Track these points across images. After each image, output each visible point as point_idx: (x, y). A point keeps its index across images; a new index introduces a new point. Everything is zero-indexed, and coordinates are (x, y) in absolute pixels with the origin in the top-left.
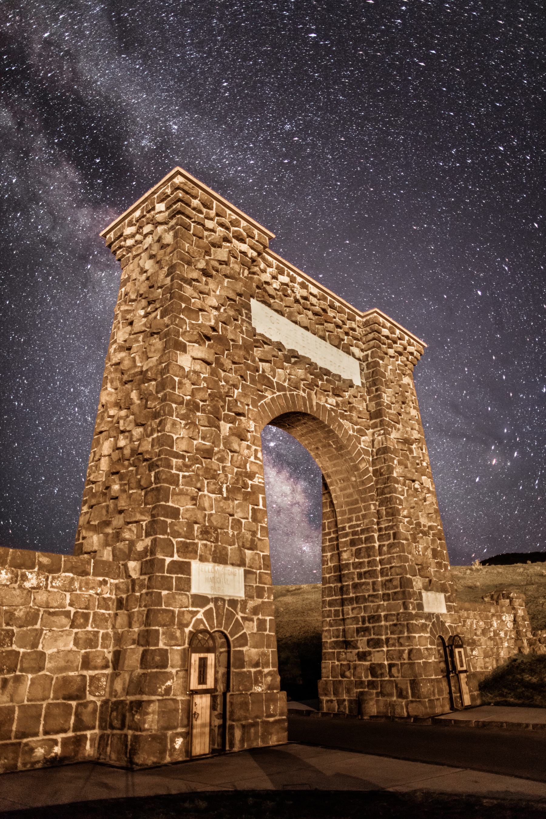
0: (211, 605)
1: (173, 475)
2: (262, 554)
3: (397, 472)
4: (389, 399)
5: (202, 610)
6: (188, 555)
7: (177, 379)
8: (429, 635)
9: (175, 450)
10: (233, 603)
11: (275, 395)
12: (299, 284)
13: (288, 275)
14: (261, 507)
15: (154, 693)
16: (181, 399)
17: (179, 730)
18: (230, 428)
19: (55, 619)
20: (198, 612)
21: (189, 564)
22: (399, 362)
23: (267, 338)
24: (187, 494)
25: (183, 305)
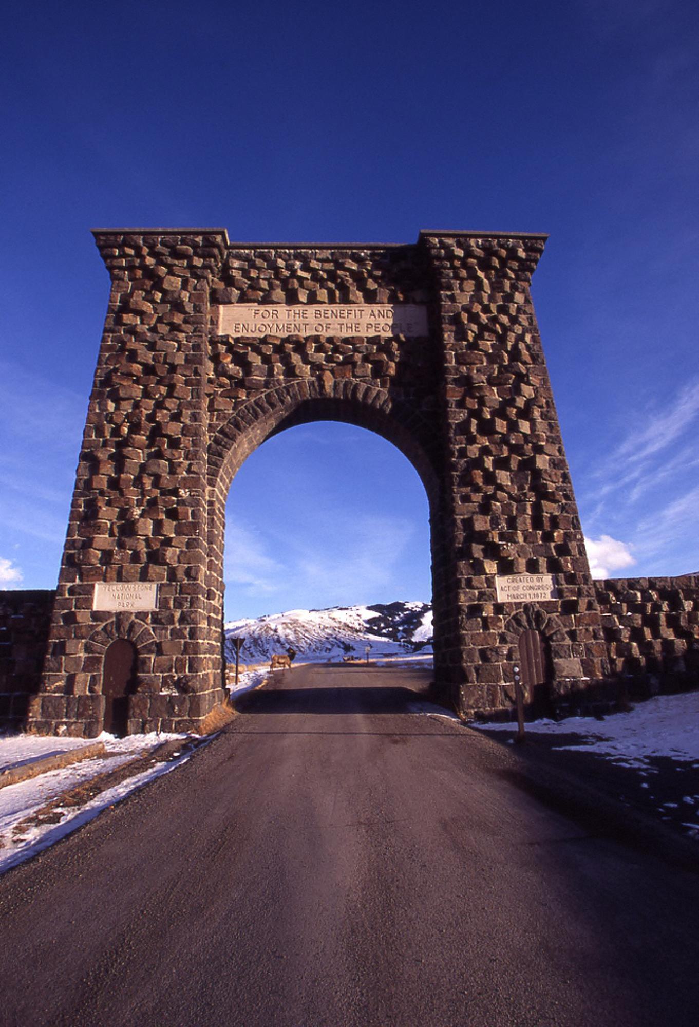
0: (114, 619)
5: (104, 624)
6: (91, 578)
8: (503, 630)
10: (142, 615)
14: (190, 519)
15: (46, 691)
16: (96, 443)
17: (64, 720)
20: (99, 625)
21: (93, 586)
23: (248, 338)
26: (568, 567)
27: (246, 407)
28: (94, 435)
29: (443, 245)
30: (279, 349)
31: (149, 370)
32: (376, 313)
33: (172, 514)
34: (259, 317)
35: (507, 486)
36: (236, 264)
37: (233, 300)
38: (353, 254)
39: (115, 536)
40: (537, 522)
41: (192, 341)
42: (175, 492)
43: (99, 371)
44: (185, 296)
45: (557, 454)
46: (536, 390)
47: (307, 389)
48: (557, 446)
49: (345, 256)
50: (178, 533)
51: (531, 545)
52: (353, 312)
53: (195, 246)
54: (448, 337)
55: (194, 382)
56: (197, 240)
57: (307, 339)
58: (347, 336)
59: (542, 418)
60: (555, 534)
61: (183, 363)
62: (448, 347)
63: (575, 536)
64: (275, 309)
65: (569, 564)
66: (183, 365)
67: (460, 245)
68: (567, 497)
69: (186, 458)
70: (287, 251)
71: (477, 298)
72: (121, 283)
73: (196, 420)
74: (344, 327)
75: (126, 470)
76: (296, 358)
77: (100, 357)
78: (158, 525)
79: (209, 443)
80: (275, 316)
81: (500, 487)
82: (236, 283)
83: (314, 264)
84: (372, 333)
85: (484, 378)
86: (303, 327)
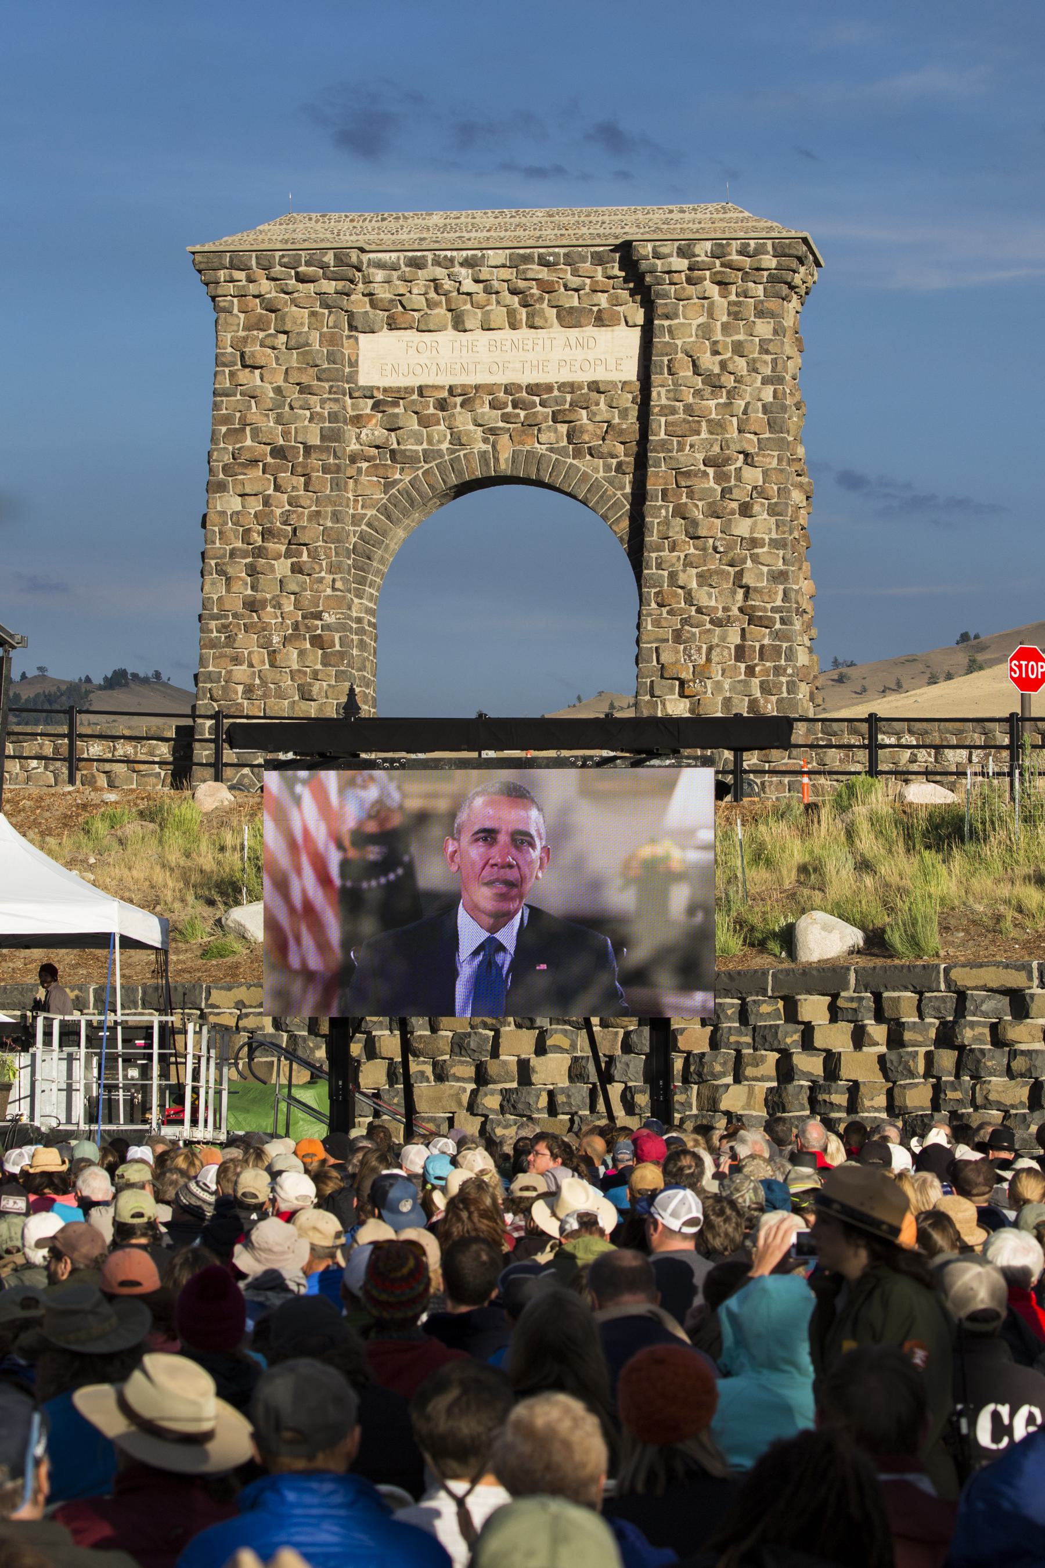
1: (211, 640)
2: (335, 702)
3: (659, 531)
4: (671, 395)
7: (216, 529)
9: (215, 611)
11: (420, 472)
12: (461, 265)
13: (437, 263)
14: (338, 648)
16: (222, 551)
18: (292, 564)
19: (146, 779)
22: (733, 297)
23: (398, 390)
24: (226, 656)
25: (224, 429)
26: (766, 707)
27: (398, 490)
28: (217, 541)
29: (657, 256)
30: (442, 405)
31: (278, 452)
32: (573, 342)
33: (317, 641)
34: (412, 352)
35: (707, 607)
36: (379, 275)
37: (376, 328)
38: (540, 256)
39: (253, 666)
40: (740, 653)
41: (327, 406)
42: (318, 616)
43: (215, 453)
44: (315, 337)
45: (781, 561)
46: (765, 473)
47: (476, 463)
48: (781, 553)
49: (527, 259)
50: (324, 664)
51: (729, 680)
52: (541, 342)
53: (324, 266)
54: (660, 396)
55: (333, 468)
56: (325, 259)
57: (477, 387)
58: (533, 381)
59: (768, 514)
60: (757, 669)
61: (318, 443)
62: (656, 410)
63: (785, 670)
64: (434, 339)
65: (769, 706)
66: (315, 447)
67: (682, 253)
68: (783, 621)
69: (331, 572)
70: (449, 254)
71: (705, 331)
72: (230, 319)
73: (338, 521)
74: (527, 365)
75: (260, 588)
76: (464, 421)
77: (214, 432)
78: (302, 653)
79: (354, 540)
80: (434, 351)
81: (699, 611)
82: (380, 304)
83: (485, 273)
84: (565, 376)
85: (700, 457)
86: (472, 367)
